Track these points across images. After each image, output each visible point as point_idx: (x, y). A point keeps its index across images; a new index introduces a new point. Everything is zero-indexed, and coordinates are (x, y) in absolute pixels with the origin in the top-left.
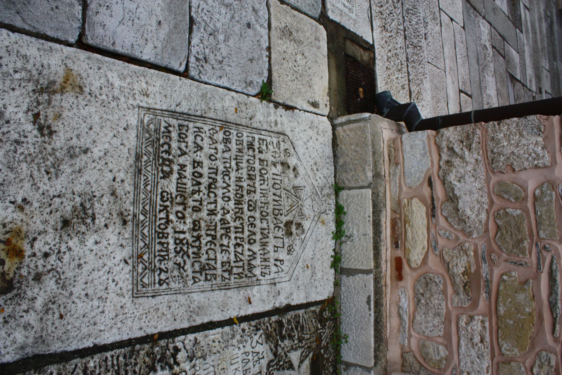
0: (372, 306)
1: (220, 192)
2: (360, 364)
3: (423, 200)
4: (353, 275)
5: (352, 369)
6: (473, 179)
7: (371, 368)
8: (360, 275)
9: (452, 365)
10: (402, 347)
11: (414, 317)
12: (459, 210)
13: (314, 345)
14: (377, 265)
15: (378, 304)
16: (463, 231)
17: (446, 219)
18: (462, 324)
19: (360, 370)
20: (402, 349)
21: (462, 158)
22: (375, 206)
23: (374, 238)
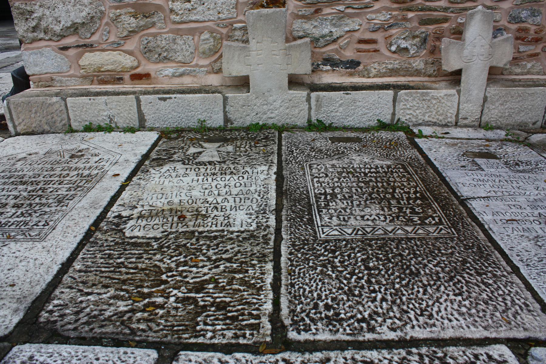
0: (168, 96)
2: (222, 108)
3: (80, 56)
5: (229, 116)
6: (56, 10)
7: (224, 96)
8: (142, 108)
9: (215, 27)
10: (209, 73)
11: (180, 62)
12: (84, 23)
14: (134, 93)
16: (101, 19)
17: (93, 34)
18: (177, 19)
19: (228, 108)
20: (210, 73)
21: (40, 19)
22: (82, 95)
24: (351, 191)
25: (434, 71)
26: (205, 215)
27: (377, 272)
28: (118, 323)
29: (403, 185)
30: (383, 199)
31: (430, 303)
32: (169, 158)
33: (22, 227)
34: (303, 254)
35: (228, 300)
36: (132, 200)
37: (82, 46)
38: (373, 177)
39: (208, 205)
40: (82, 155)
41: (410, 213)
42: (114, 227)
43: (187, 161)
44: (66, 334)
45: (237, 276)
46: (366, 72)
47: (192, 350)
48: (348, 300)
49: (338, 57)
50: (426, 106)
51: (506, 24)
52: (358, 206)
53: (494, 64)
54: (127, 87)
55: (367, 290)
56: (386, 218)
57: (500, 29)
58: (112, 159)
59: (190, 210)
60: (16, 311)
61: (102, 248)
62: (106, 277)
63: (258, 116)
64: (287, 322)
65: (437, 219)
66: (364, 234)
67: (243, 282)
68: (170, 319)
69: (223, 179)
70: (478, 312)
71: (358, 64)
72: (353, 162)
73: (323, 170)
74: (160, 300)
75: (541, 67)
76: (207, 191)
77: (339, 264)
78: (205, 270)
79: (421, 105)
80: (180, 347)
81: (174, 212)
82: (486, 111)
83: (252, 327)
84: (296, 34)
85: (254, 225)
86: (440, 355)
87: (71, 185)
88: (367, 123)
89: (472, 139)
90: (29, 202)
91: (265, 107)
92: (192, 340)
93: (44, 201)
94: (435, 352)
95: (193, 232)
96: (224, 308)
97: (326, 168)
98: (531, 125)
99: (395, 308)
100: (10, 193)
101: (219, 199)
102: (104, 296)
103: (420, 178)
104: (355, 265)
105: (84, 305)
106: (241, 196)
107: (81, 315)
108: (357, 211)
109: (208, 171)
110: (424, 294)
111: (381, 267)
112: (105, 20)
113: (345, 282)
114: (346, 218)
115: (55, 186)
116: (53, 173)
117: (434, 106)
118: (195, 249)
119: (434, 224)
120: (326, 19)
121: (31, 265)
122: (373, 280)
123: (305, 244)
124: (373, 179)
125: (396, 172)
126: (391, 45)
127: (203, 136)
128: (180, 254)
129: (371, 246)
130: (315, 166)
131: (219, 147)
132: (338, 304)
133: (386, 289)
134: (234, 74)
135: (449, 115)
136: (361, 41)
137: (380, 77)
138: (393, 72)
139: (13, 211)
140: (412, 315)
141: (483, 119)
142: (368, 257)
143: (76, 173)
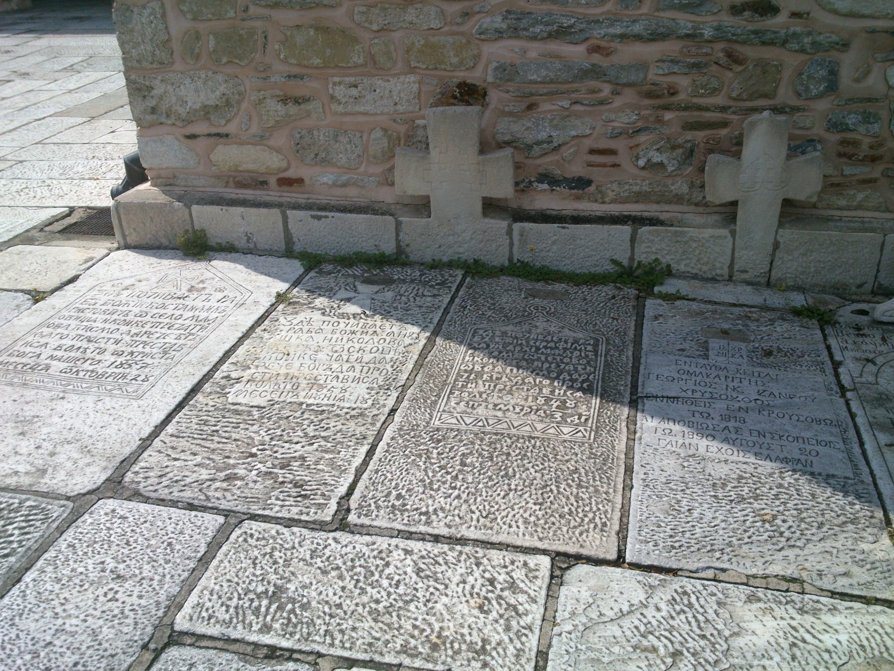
0: (323, 214)
1: (104, 334)
2: (394, 235)
6: (182, 87)
7: (396, 220)
8: (290, 227)
10: (380, 184)
12: (217, 106)
14: (279, 205)
16: (239, 102)
17: (228, 121)
18: (340, 109)
19: (401, 234)
20: (382, 184)
22: (212, 203)
23: (246, 206)
24: (504, 371)
26: (321, 385)
27: (470, 469)
28: (196, 490)
29: (576, 370)
30: (536, 385)
32: (310, 303)
33: (120, 381)
38: (546, 354)
39: (330, 373)
40: (204, 288)
41: (557, 407)
42: (218, 389)
44: (147, 494)
45: (327, 456)
46: (600, 196)
47: (256, 521)
48: (424, 493)
49: (559, 172)
50: (680, 251)
51: (822, 133)
52: (500, 391)
53: (790, 195)
54: (272, 195)
55: (447, 486)
56: (522, 410)
57: (813, 140)
60: (105, 468)
61: (200, 413)
62: (197, 444)
63: (442, 249)
65: (583, 420)
66: (484, 426)
67: (332, 463)
68: (246, 491)
69: (360, 341)
71: (589, 183)
74: (241, 472)
75: (881, 200)
76: (336, 355)
77: (435, 456)
78: (298, 447)
79: (673, 249)
80: (246, 517)
81: (289, 377)
83: (320, 506)
84: (500, 138)
85: (370, 402)
86: (480, 555)
87: (182, 332)
90: (130, 349)
91: (451, 237)
92: (260, 512)
93: (147, 349)
94: (477, 552)
95: (301, 404)
97: (493, 336)
98: (854, 289)
99: (464, 507)
100: (110, 336)
102: (190, 463)
104: (452, 458)
105: (168, 470)
107: (164, 479)
108: (495, 397)
110: (504, 498)
111: (477, 464)
112: (244, 105)
113: (431, 474)
114: (476, 404)
115: (163, 331)
116: (162, 311)
117: (694, 251)
118: (297, 423)
119: (577, 425)
120: (543, 119)
121: (123, 425)
122: (460, 477)
123: (413, 430)
124: (543, 358)
126: (638, 158)
127: (364, 271)
128: (279, 427)
129: (482, 440)
130: (481, 332)
131: (377, 292)
132: (410, 496)
133: (467, 488)
134: (410, 192)
135: (718, 265)
136: (592, 152)
137: (620, 203)
138: (639, 197)
141: (773, 273)
142: (471, 452)
143: (191, 314)
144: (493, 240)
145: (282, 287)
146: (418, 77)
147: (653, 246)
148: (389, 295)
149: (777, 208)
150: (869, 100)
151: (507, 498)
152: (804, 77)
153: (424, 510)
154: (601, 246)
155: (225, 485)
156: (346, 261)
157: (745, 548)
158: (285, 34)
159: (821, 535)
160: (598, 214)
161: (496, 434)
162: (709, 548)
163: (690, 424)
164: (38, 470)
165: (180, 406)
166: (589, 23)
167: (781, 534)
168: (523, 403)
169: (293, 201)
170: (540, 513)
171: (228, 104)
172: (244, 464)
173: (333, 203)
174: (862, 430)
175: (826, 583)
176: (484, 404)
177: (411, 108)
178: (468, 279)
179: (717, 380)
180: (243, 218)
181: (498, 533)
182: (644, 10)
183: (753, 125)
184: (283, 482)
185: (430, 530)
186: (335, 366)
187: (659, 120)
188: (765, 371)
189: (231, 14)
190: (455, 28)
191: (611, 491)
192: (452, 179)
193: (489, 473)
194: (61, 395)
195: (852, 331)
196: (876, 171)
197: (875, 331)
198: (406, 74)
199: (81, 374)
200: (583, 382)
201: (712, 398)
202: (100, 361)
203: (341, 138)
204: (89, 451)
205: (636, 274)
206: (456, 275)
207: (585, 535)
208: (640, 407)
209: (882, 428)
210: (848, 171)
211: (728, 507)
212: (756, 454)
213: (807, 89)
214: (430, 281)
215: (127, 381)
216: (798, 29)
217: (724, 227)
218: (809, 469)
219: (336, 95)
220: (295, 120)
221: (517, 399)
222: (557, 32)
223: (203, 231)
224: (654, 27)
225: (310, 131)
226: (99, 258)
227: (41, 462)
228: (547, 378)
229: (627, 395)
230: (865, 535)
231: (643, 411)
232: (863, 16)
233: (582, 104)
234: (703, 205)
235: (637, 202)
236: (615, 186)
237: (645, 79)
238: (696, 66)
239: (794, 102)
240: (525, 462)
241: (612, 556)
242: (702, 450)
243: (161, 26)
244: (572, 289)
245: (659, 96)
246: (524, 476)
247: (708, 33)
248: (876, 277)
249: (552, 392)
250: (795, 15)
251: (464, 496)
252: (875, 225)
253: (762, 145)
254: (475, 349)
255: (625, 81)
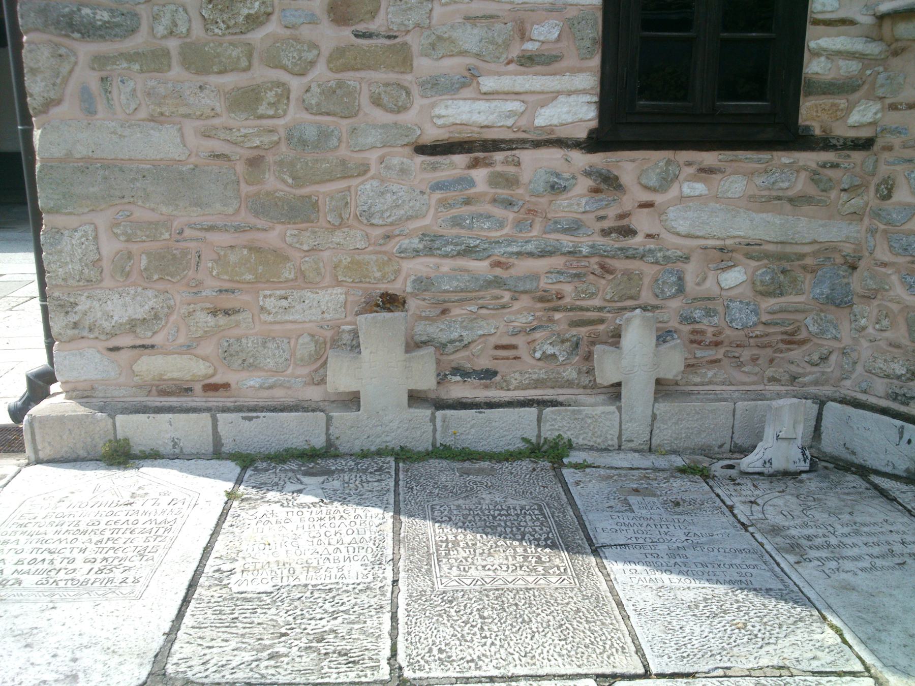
0: (254, 414)
1: (63, 545)
2: (324, 429)
4: (221, 439)
6: (109, 302)
7: (327, 415)
12: (145, 319)
13: (290, 474)
14: (208, 410)
15: (254, 409)
16: (167, 316)
17: (154, 333)
18: (270, 318)
19: (331, 428)
20: (309, 384)
23: (174, 413)
25: (590, 381)
27: (490, 620)
31: (535, 646)
32: (262, 498)
33: (108, 584)
34: (420, 605)
35: (348, 648)
36: (229, 551)
37: (140, 346)
39: (318, 556)
40: (146, 494)
41: (536, 562)
43: (286, 504)
45: (356, 626)
50: (578, 427)
51: (677, 325)
52: (481, 554)
54: (198, 400)
55: (478, 636)
56: (508, 568)
57: (670, 331)
58: (188, 499)
59: (299, 562)
64: (404, 664)
65: (562, 569)
67: (363, 631)
69: (333, 525)
70: (577, 653)
71: (495, 373)
72: (482, 501)
73: (446, 513)
74: (282, 650)
75: (725, 376)
77: (454, 614)
78: (324, 622)
79: (573, 426)
81: (281, 564)
82: (655, 432)
84: (418, 339)
87: (147, 535)
88: (506, 448)
89: (638, 469)
91: (379, 428)
93: (120, 554)
95: (306, 586)
96: (346, 654)
97: (450, 509)
98: (716, 449)
99: (502, 651)
100: (72, 546)
101: (331, 549)
103: (556, 522)
105: (207, 657)
106: (355, 545)
107: (208, 666)
109: (314, 515)
111: (495, 616)
112: (173, 318)
114: (467, 568)
116: (115, 519)
117: (589, 426)
119: (559, 575)
122: (486, 628)
123: (423, 596)
124: (503, 524)
125: (530, 514)
126: (535, 351)
128: (296, 607)
129: (487, 596)
130: (438, 507)
131: (323, 483)
133: (497, 636)
135: (609, 437)
136: (497, 347)
138: (538, 384)
139: (88, 566)
140: (516, 656)
141: (653, 441)
143: (146, 518)
144: (418, 428)
145: (229, 486)
146: (344, 290)
147: (556, 425)
148: (337, 484)
149: (652, 387)
150: (709, 299)
151: (534, 639)
152: (660, 282)
153: (469, 658)
154: (512, 427)
155: (272, 663)
156: (280, 458)
157: (735, 649)
158: (218, 253)
159: (784, 633)
160: (507, 399)
161: (497, 590)
162: (709, 654)
163: (647, 564)
164: (68, 676)
165: (186, 601)
166: (490, 243)
167: (756, 636)
168: (506, 562)
169: (221, 404)
170: (569, 647)
171: (156, 317)
172: (280, 643)
173: (261, 404)
174: (774, 553)
175: (805, 666)
176: (473, 567)
177: (337, 316)
178: (401, 465)
179: (649, 528)
180: (171, 425)
181: (542, 667)
182: (535, 233)
183: (629, 320)
184: (326, 654)
185: (484, 674)
186: (320, 549)
187: (551, 320)
188: (682, 518)
189: (167, 236)
190: (378, 248)
191: (614, 622)
192: (381, 376)
193: (509, 622)
194: (51, 605)
195: (729, 482)
196: (719, 353)
197: (745, 480)
198: (333, 287)
199: (62, 584)
200: (546, 540)
201: (652, 542)
202: (75, 570)
203: (270, 345)
204: (113, 652)
205: (543, 449)
206: (389, 462)
207: (612, 658)
208: (602, 555)
209: (787, 552)
210: (699, 354)
211: (708, 622)
212: (708, 580)
213: (663, 291)
214: (367, 469)
215: (117, 584)
216: (652, 246)
217: (611, 404)
218: (751, 586)
219: (267, 306)
220: (224, 330)
221: (498, 559)
222: (464, 250)
223: (126, 440)
224: (543, 246)
225: (238, 339)
226: (12, 474)
227: (66, 668)
228: (515, 539)
229: (587, 546)
230: (814, 628)
231: (606, 558)
232: (698, 237)
233: (488, 309)
234: (593, 386)
235: (535, 388)
236: (517, 375)
237: (538, 287)
238: (577, 276)
239: (654, 302)
240: (534, 608)
241: (641, 671)
242: (667, 583)
243: (92, 247)
244: (497, 466)
245: (550, 301)
246: (539, 619)
247: (585, 250)
248: (732, 438)
249: (525, 551)
250: (649, 236)
251: (497, 642)
252: (725, 396)
253: (637, 336)
254: (441, 522)
255: (522, 289)
